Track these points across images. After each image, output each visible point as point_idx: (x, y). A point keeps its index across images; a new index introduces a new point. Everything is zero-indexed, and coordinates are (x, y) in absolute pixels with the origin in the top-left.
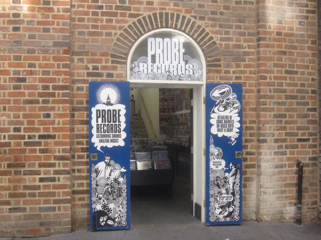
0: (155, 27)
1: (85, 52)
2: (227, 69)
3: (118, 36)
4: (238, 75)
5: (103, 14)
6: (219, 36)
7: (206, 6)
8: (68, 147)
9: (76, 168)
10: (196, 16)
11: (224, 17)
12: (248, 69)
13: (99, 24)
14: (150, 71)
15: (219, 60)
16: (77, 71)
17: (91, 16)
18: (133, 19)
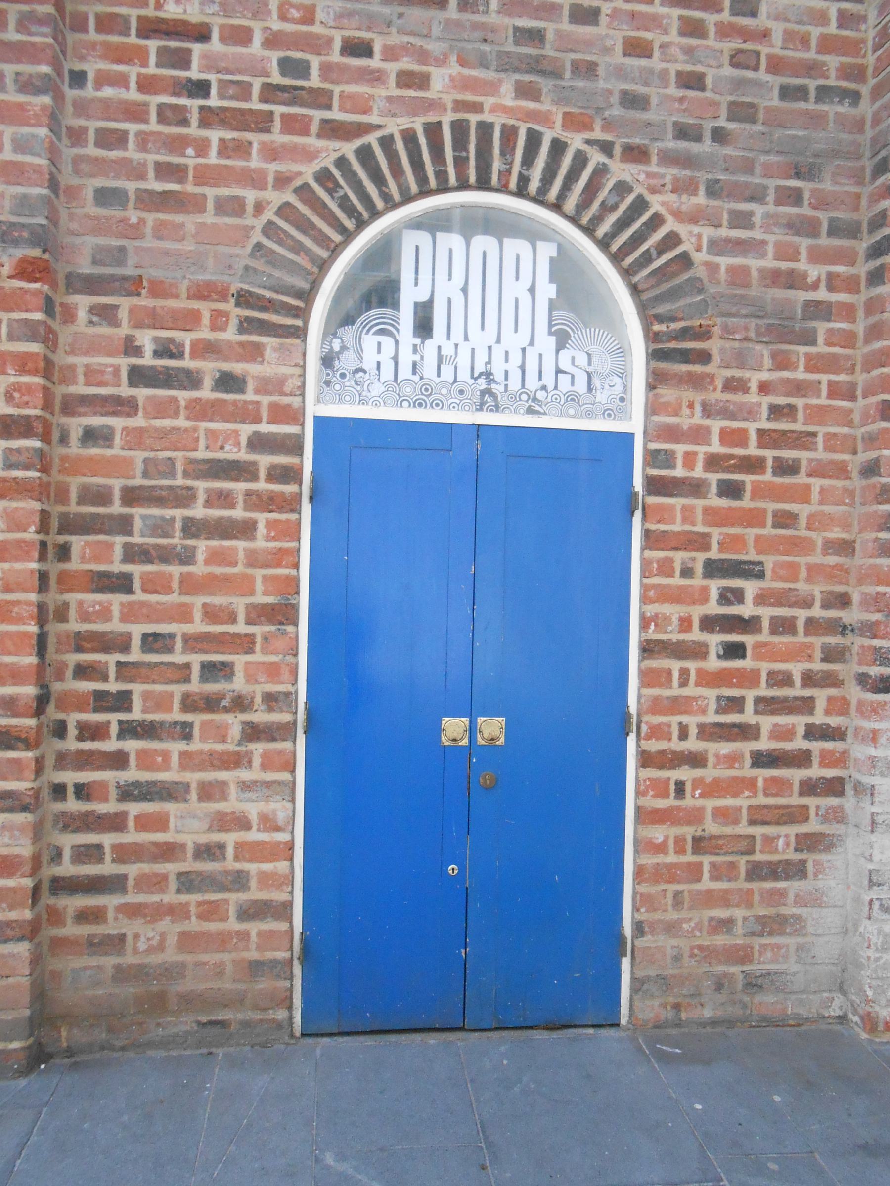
0: (433, 183)
1: (125, 278)
2: (738, 373)
3: (269, 215)
4: (782, 401)
5: (208, 117)
6: (707, 233)
7: (654, 101)
8: (29, 691)
9: (70, 777)
10: (612, 144)
11: (728, 151)
12: (824, 378)
13: (190, 159)
14: (405, 372)
15: (703, 334)
16: (85, 360)
17: (153, 125)
18: (337, 144)
